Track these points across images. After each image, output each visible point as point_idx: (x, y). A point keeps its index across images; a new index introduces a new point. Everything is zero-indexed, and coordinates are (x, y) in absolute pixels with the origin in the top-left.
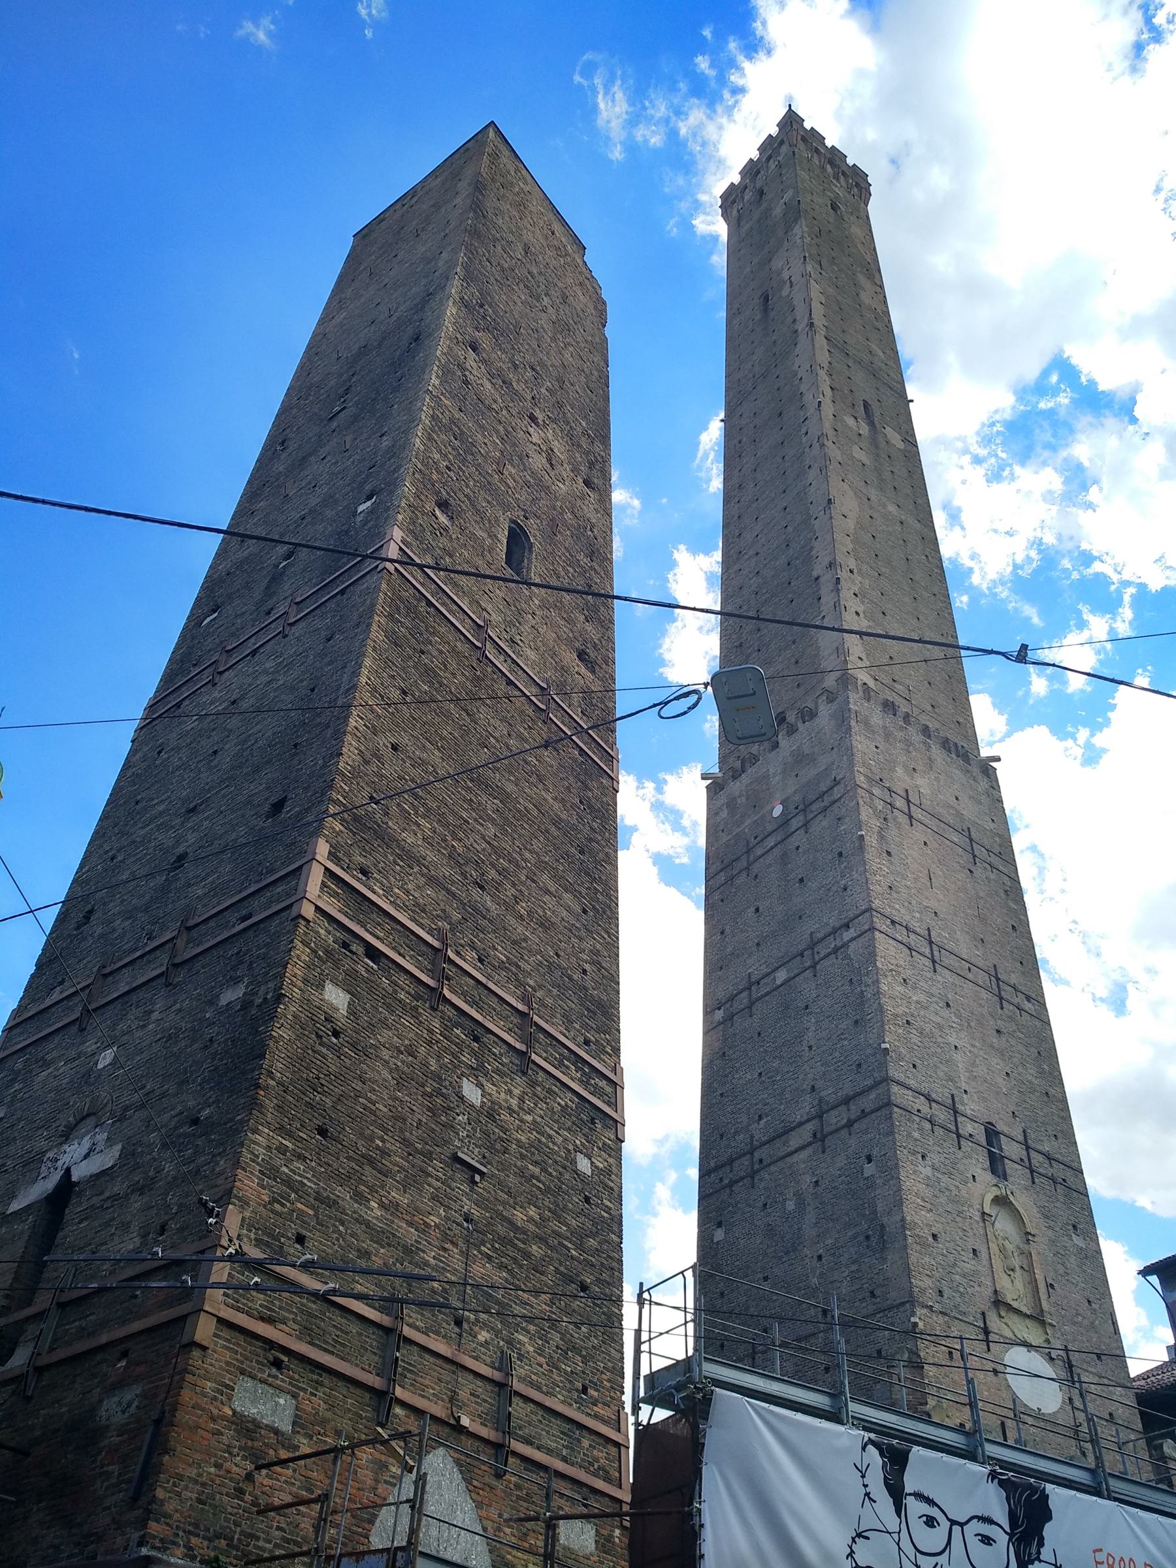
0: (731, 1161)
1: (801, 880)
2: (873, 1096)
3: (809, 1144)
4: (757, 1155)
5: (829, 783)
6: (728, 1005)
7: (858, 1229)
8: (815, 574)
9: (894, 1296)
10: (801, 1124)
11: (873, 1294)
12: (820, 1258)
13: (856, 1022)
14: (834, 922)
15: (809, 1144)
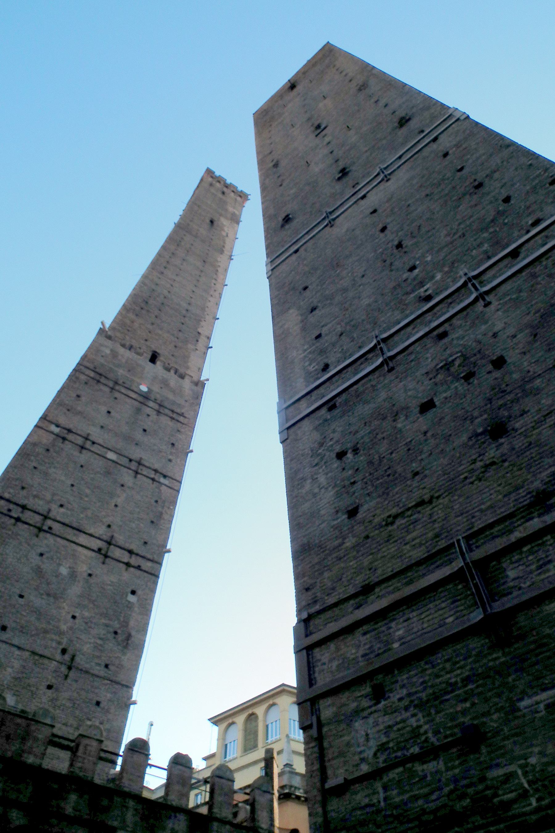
0: (24, 507)
1: (145, 430)
2: (149, 564)
3: (93, 550)
4: (49, 523)
5: (178, 411)
6: (66, 431)
7: (111, 623)
8: (200, 330)
9: (121, 678)
10: (91, 535)
11: (107, 666)
12: (74, 617)
13: (152, 522)
14: (156, 466)
15: (93, 550)
